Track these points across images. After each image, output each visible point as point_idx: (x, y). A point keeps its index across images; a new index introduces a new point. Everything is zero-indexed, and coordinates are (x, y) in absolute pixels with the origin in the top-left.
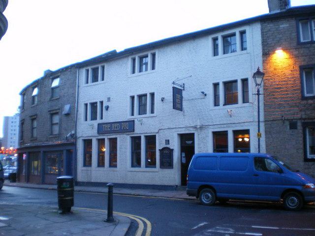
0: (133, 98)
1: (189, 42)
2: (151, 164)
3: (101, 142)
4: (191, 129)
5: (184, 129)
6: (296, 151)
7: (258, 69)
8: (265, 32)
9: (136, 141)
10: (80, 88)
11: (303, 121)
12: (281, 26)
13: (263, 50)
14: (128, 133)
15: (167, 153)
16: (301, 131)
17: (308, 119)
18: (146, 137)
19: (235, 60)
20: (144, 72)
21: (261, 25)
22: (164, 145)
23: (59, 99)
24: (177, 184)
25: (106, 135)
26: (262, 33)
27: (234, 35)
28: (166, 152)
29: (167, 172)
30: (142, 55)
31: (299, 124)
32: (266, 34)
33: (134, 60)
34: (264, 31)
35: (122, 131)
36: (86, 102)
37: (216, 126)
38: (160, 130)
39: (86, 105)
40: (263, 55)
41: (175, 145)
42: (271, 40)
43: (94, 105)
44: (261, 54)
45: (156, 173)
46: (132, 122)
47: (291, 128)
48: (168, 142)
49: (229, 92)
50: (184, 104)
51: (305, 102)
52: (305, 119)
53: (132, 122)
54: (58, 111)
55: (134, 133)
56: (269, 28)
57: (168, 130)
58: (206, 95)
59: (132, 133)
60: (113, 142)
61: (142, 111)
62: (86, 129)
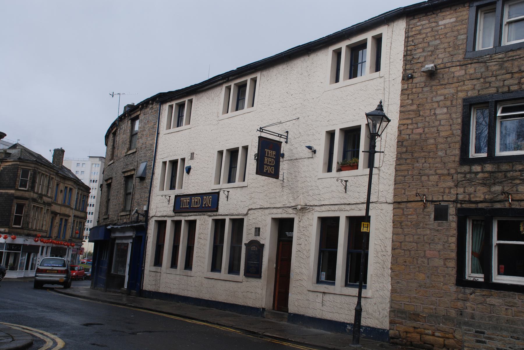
0: (221, 153)
1: (302, 59)
2: (233, 269)
3: (177, 224)
4: (290, 210)
5: (280, 211)
6: (442, 263)
7: (380, 107)
8: (413, 36)
9: (219, 224)
10: (160, 135)
11: (459, 206)
12: (441, 23)
13: (405, 70)
14: (209, 214)
15: (256, 248)
16: (454, 225)
17: (470, 202)
18: (233, 221)
19: (361, 90)
20: (184, 127)
21: (408, 24)
22: (252, 237)
23: (136, 152)
24: (263, 307)
25: (183, 214)
26: (407, 37)
27: (363, 45)
28: (254, 248)
29: (254, 282)
30: (238, 83)
31: (452, 211)
32: (413, 41)
33: (229, 88)
34: (411, 34)
35: (202, 210)
36: (164, 160)
37: (323, 208)
38: (249, 210)
39: (165, 163)
40: (403, 79)
41: (267, 238)
42: (421, 50)
43: (174, 163)
44: (401, 78)
45: (240, 284)
46: (215, 196)
47: (436, 219)
48: (258, 231)
49: (350, 147)
50: (284, 166)
51: (466, 168)
52: (462, 202)
53: (215, 196)
54: (133, 173)
55: (218, 213)
56: (420, 28)
57: (259, 210)
58: (315, 152)
59: (215, 213)
60: (192, 224)
61: (231, 179)
62: (161, 204)
